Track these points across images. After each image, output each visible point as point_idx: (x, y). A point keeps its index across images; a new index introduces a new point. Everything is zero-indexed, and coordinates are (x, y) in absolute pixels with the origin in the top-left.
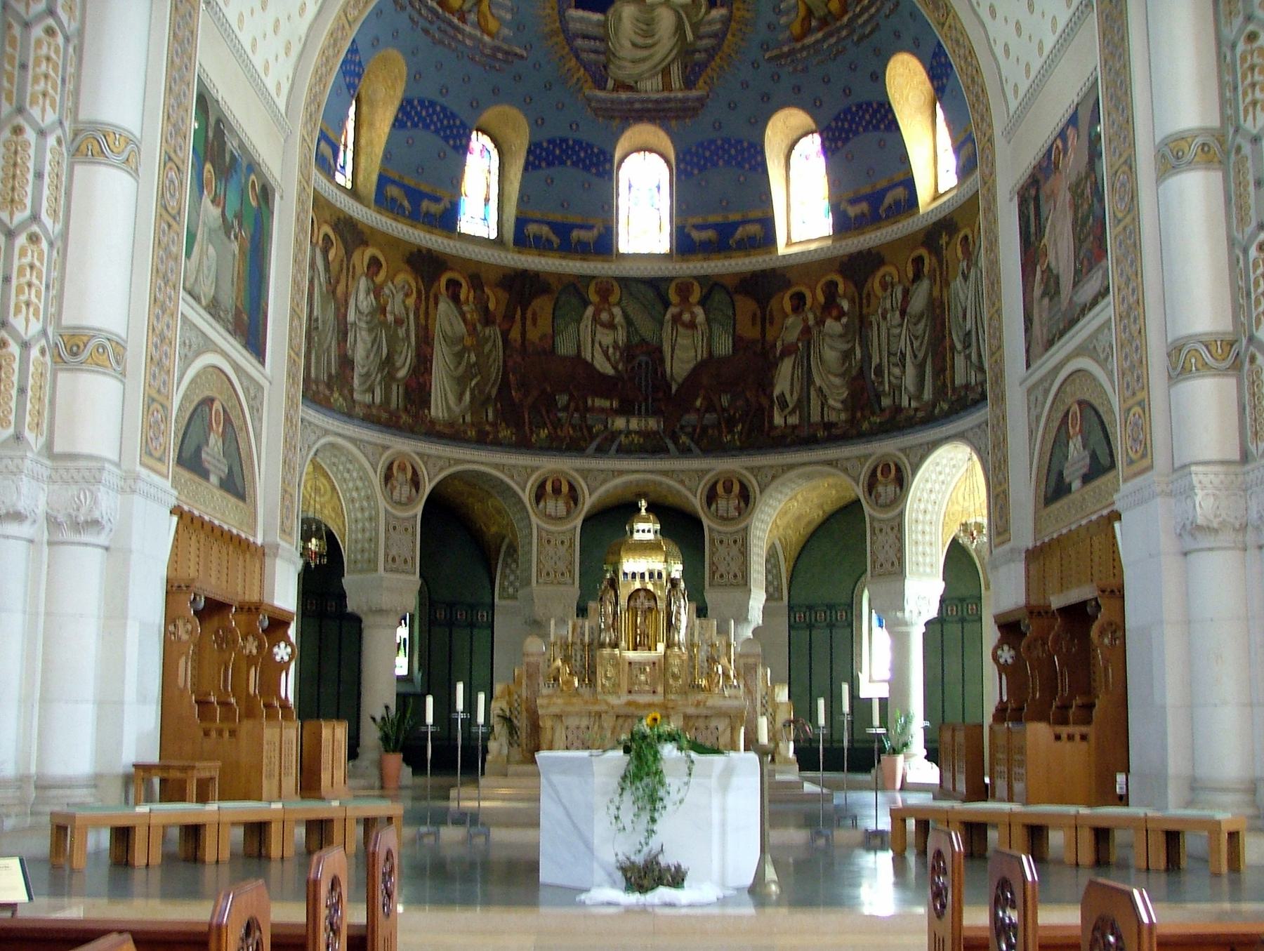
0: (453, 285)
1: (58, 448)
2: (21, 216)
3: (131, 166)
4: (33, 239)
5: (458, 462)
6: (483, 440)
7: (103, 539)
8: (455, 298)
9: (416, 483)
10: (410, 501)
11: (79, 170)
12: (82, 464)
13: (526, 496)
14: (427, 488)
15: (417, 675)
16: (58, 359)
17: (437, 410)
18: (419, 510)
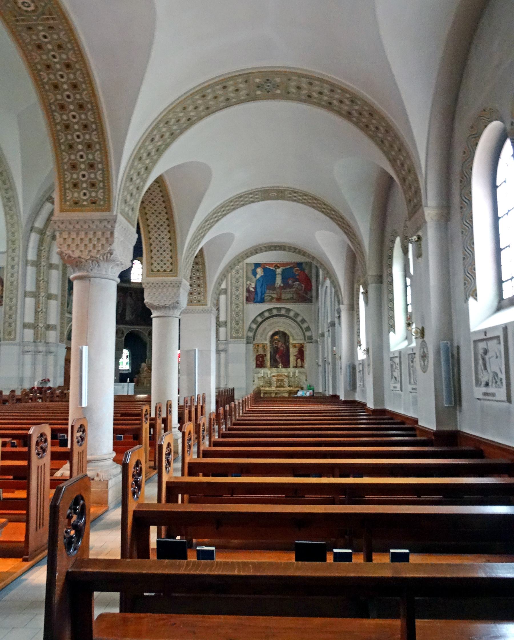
0: (131, 293)
1: (47, 341)
2: (40, 309)
3: (56, 299)
4: (42, 312)
5: (132, 328)
6: (138, 324)
7: (53, 354)
8: (131, 296)
9: (123, 333)
10: (121, 337)
11: (49, 301)
12: (50, 344)
13: (147, 335)
14: (126, 334)
15: (130, 369)
16: (46, 329)
17: (127, 318)
18: (123, 338)
